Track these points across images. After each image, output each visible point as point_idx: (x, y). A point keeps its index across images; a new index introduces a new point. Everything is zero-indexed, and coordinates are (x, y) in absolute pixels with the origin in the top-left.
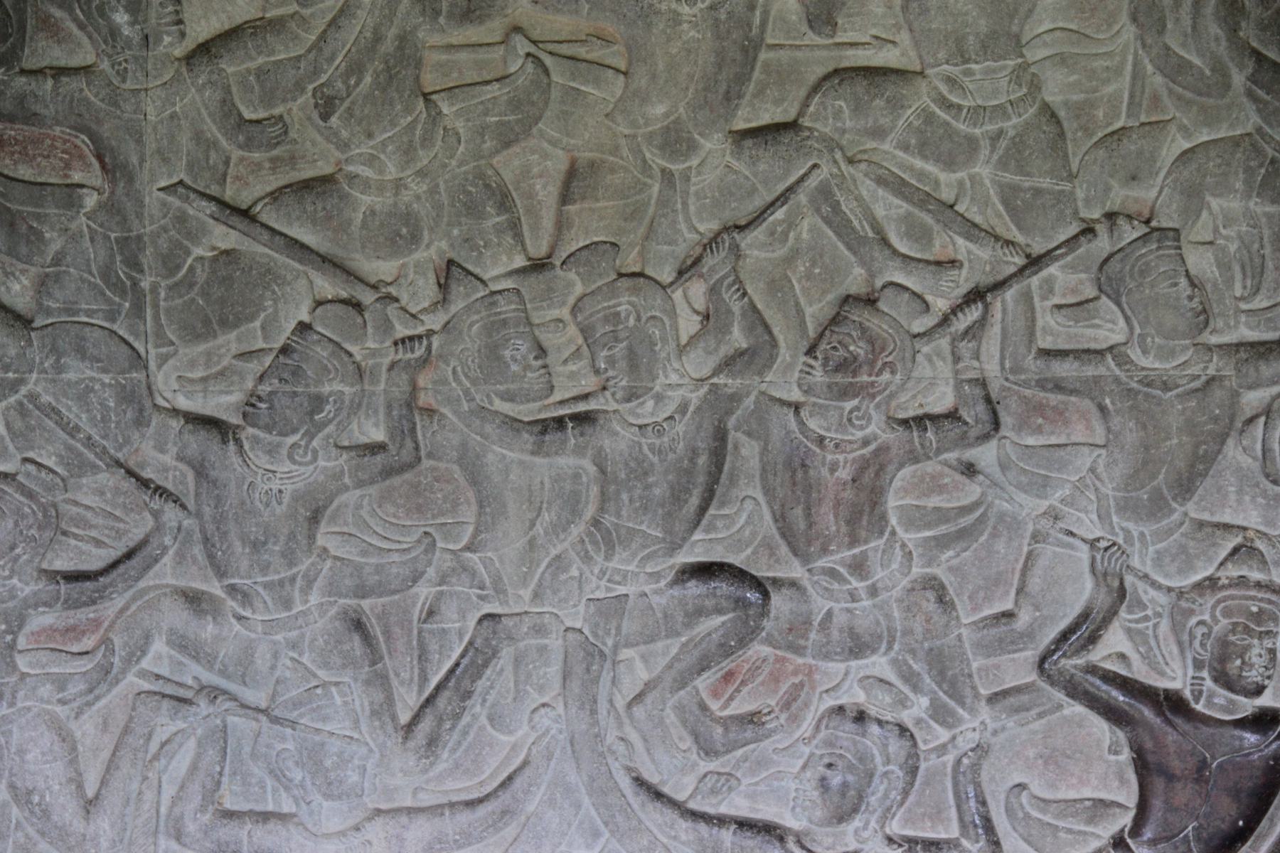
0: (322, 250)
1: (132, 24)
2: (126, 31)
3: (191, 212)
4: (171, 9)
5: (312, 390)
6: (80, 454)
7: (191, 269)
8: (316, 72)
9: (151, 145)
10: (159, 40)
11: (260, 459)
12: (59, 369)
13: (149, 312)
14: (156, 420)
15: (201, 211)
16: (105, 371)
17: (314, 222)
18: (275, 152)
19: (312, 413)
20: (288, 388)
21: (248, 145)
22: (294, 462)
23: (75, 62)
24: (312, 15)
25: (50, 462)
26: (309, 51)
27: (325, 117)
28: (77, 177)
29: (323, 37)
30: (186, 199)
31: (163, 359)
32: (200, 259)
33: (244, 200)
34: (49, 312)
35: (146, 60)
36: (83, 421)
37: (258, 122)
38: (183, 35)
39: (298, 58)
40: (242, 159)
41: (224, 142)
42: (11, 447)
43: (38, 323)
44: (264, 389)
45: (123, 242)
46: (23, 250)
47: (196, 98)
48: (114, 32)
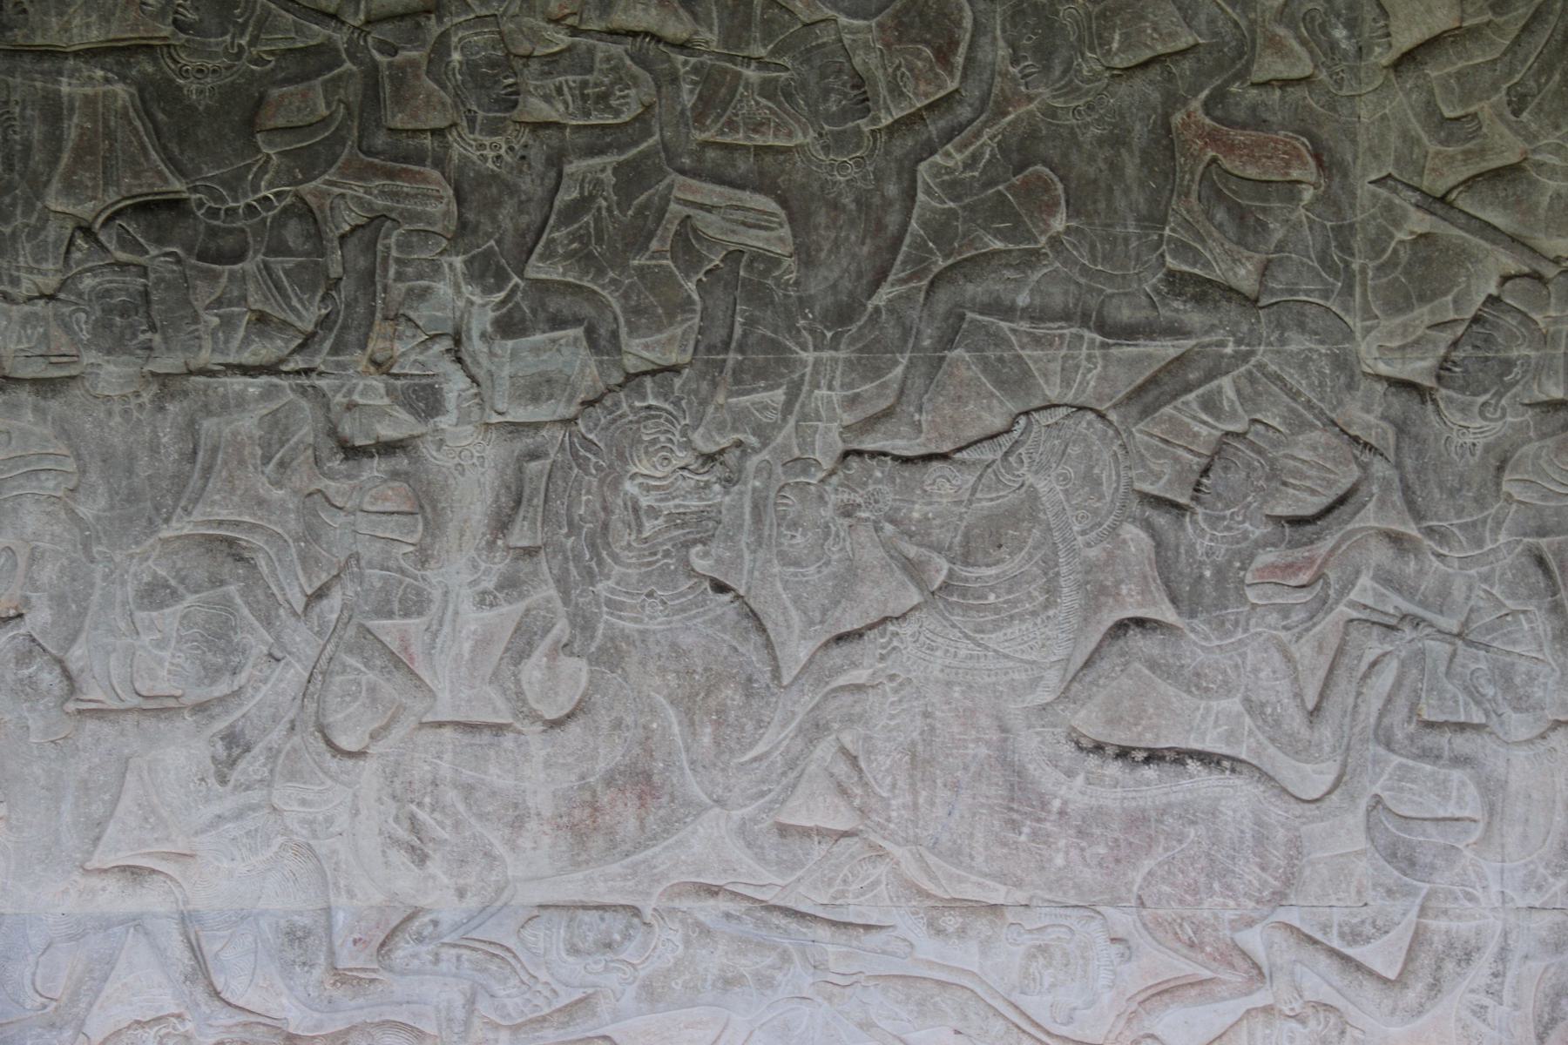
0: (1510, 230)
1: (1349, 38)
2: (1344, 45)
3: (1397, 201)
4: (1382, 23)
5: (1502, 354)
6: (1301, 415)
7: (1395, 251)
8: (1510, 74)
9: (1363, 143)
10: (1371, 51)
11: (1456, 418)
12: (1283, 341)
13: (1358, 290)
14: (1364, 384)
15: (1405, 200)
16: (1322, 342)
17: (1505, 207)
18: (1469, 146)
19: (1501, 375)
20: (1480, 354)
21: (1445, 142)
22: (1485, 418)
23: (1296, 73)
24: (1506, 22)
25: (1275, 423)
26: (1504, 54)
27: (1516, 113)
28: (1295, 174)
29: (1517, 42)
30: (1395, 191)
31: (1368, 330)
32: (1402, 242)
33: (1440, 188)
34: (1273, 293)
35: (1359, 69)
36: (1303, 386)
37: (1457, 119)
38: (1390, 45)
39: (1494, 61)
40: (1438, 153)
41: (1425, 139)
42: (1240, 410)
43: (1264, 301)
44: (1458, 355)
45: (1338, 230)
46: (1251, 239)
47: (1402, 102)
48: (1333, 46)
